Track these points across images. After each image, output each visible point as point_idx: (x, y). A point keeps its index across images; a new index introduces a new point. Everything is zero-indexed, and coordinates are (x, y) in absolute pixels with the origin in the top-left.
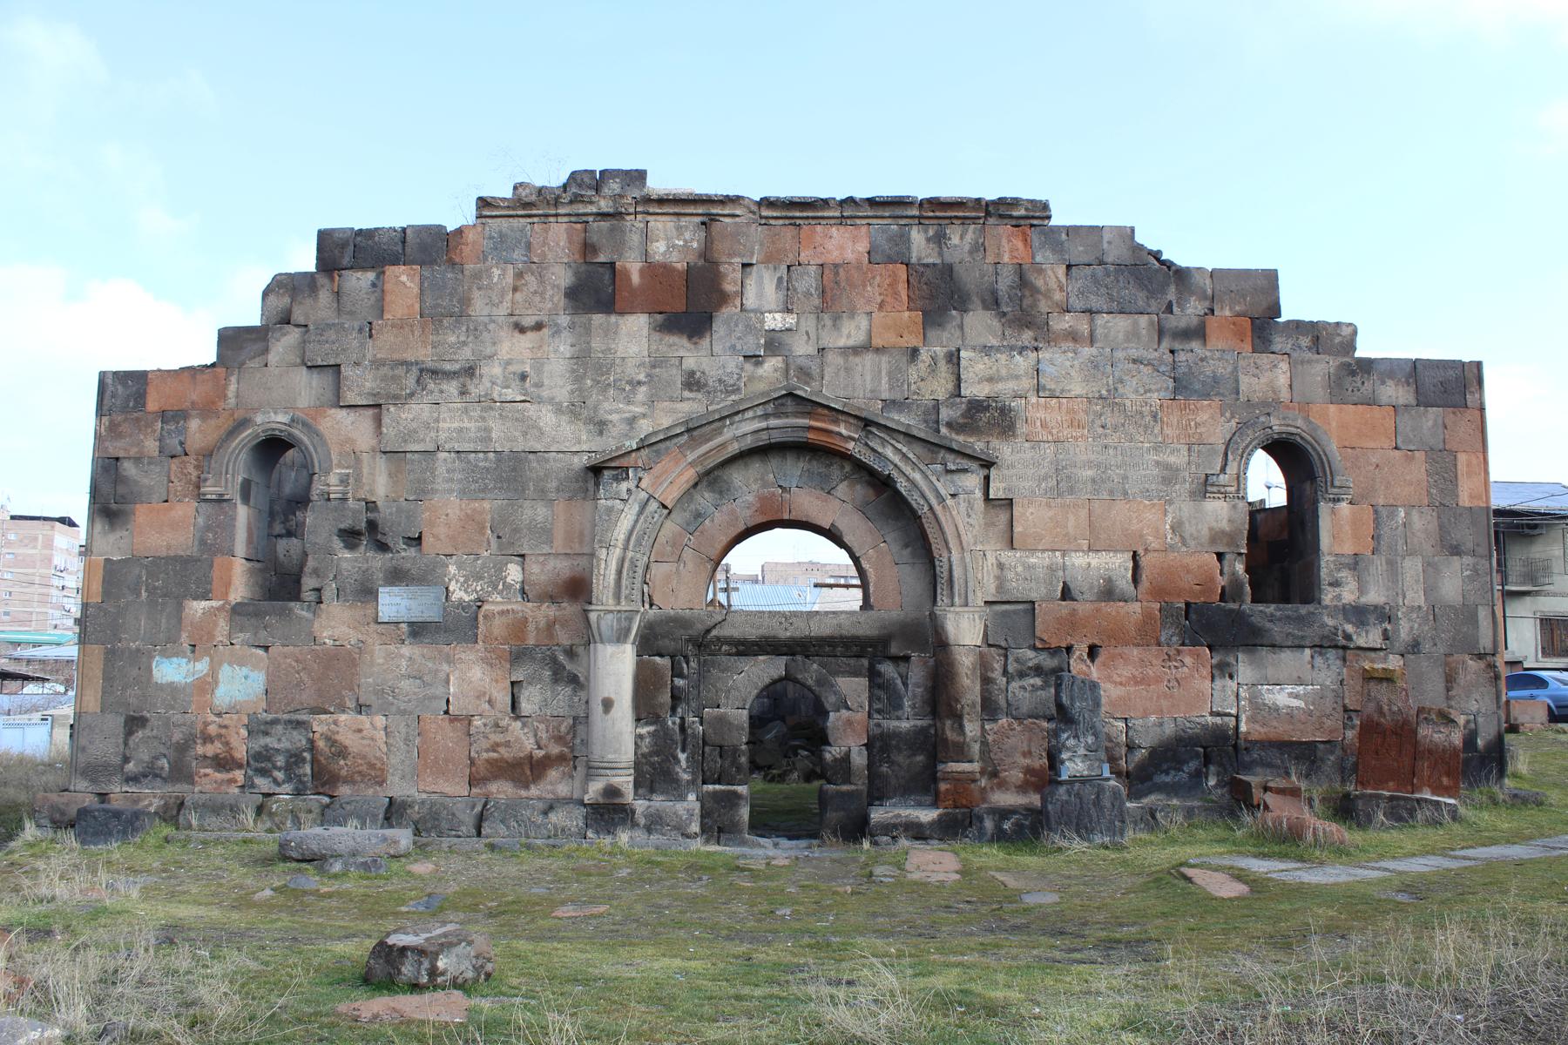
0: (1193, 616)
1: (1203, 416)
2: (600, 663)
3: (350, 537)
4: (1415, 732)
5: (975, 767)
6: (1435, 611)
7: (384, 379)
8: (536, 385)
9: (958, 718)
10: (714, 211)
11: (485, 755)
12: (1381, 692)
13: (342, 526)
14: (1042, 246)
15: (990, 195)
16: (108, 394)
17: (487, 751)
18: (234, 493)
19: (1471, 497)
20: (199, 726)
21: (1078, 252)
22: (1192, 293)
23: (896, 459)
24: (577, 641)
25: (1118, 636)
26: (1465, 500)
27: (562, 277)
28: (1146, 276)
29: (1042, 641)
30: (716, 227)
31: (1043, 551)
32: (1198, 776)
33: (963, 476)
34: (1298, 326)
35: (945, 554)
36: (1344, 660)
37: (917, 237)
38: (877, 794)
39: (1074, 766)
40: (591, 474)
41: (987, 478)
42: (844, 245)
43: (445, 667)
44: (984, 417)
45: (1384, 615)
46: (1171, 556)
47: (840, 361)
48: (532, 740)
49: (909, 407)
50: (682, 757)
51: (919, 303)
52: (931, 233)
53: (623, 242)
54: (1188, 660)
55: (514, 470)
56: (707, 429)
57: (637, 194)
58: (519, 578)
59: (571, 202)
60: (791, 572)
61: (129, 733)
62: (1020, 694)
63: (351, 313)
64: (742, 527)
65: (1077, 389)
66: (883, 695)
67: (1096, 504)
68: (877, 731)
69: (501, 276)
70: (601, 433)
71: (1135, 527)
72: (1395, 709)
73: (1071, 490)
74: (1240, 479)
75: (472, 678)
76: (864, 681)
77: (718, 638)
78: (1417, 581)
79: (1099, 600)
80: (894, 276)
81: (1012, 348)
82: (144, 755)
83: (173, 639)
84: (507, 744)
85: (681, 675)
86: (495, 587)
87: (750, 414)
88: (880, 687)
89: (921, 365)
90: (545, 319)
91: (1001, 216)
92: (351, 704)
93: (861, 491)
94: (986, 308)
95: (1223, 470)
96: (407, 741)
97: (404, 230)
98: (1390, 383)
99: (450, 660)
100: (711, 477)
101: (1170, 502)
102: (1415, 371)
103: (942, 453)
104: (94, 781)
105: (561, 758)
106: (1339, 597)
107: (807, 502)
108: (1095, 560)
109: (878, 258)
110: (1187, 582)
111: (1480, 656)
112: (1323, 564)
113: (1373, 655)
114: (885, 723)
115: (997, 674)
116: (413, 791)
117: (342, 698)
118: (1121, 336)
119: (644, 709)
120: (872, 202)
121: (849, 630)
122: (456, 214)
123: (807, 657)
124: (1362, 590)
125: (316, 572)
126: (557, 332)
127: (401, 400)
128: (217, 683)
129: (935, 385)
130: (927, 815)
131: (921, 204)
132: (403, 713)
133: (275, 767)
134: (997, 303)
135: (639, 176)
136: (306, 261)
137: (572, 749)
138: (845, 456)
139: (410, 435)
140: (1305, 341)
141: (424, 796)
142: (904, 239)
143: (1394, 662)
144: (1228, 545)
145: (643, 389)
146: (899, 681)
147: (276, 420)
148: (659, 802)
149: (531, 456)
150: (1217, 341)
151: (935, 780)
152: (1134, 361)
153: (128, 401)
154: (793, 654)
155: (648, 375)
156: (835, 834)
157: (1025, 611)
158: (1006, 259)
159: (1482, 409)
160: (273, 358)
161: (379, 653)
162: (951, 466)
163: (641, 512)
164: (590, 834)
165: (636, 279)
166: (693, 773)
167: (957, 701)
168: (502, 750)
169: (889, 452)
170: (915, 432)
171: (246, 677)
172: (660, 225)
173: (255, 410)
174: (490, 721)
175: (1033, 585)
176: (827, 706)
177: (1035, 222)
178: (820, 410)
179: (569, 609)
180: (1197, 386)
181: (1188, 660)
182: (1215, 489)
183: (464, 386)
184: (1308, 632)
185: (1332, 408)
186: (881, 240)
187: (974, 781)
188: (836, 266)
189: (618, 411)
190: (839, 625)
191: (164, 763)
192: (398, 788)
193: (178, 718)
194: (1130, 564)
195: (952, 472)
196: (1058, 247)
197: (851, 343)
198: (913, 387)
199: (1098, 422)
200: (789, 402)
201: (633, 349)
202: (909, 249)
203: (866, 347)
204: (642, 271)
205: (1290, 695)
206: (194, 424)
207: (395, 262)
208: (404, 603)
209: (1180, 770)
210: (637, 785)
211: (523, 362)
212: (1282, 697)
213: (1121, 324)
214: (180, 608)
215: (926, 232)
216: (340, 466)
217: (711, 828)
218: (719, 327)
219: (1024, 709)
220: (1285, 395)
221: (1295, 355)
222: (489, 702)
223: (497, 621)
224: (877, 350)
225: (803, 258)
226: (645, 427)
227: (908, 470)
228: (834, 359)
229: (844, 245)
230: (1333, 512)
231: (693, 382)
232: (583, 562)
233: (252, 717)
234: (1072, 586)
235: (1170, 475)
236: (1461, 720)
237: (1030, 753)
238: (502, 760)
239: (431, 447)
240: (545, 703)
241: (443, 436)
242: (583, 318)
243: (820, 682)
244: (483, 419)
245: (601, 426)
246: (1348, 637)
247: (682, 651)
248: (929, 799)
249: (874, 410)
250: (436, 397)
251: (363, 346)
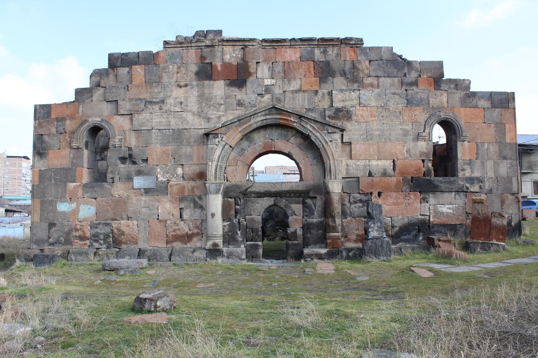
0: (414, 182)
1: (417, 113)
2: (210, 201)
3: (123, 160)
4: (491, 220)
5: (340, 234)
6: (497, 179)
7: (133, 105)
8: (186, 105)
9: (333, 218)
10: (246, 44)
11: (171, 233)
12: (479, 207)
13: (120, 156)
14: (361, 54)
15: (342, 36)
16: (38, 112)
17: (172, 232)
18: (82, 146)
19: (510, 139)
20: (74, 226)
21: (373, 56)
22: (413, 70)
23: (311, 129)
24: (202, 194)
25: (388, 189)
26: (508, 140)
27: (194, 68)
28: (397, 64)
29: (363, 191)
30: (247, 49)
31: (362, 160)
32: (416, 236)
33: (334, 135)
34: (450, 81)
35: (328, 162)
36: (466, 196)
37: (317, 52)
38: (306, 243)
39: (373, 233)
40: (205, 136)
41: (342, 135)
42: (291, 55)
43: (157, 204)
44: (341, 114)
45: (480, 180)
46: (406, 161)
47: (291, 95)
48: (187, 228)
49: (315, 111)
50: (239, 232)
51: (318, 75)
52: (322, 50)
53: (215, 56)
54: (412, 197)
55: (179, 135)
56: (245, 120)
57: (219, 38)
58: (181, 172)
59: (196, 42)
60: (275, 168)
61: (50, 229)
62: (355, 209)
63: (121, 82)
64: (258, 153)
65: (373, 104)
66: (308, 210)
67: (380, 143)
68: (306, 222)
69: (172, 68)
70: (208, 122)
71: (394, 151)
72: (484, 212)
73: (371, 139)
74: (430, 134)
75: (166, 207)
76: (301, 206)
77: (250, 192)
78: (491, 169)
79: (381, 176)
80: (309, 65)
81: (350, 90)
82: (55, 236)
83: (63, 196)
84: (179, 229)
85: (238, 205)
86: (173, 176)
87: (260, 114)
88: (306, 207)
89: (319, 96)
90: (188, 83)
91: (346, 44)
92: (125, 217)
93: (299, 140)
94: (341, 76)
95: (424, 131)
96: (145, 229)
97: (138, 53)
98: (482, 100)
99: (159, 201)
100: (247, 136)
101: (406, 142)
102: (491, 96)
103: (327, 126)
104: (39, 245)
105: (198, 234)
106: (464, 174)
107: (280, 144)
108: (380, 163)
109: (303, 59)
110: (412, 170)
111: (513, 194)
112: (459, 163)
113: (476, 194)
114: (308, 220)
115: (347, 202)
116: (147, 246)
117: (122, 215)
118: (388, 85)
119: (226, 217)
120: (301, 40)
121: (295, 188)
122: (156, 47)
123: (281, 197)
124: (472, 172)
125: (112, 172)
126: (192, 87)
127: (139, 112)
128: (79, 211)
129: (324, 103)
130: (323, 251)
131: (318, 40)
132: (143, 219)
133: (100, 239)
134: (345, 74)
135: (220, 32)
136: (104, 64)
137: (201, 231)
138: (293, 128)
139: (142, 124)
140: (453, 86)
141: (151, 248)
142: (312, 52)
143: (483, 197)
144: (426, 157)
145: (223, 106)
146: (313, 205)
147: (96, 120)
148: (231, 248)
149: (185, 130)
150: (422, 86)
151: (326, 239)
152: (393, 94)
153: (44, 114)
154: (276, 197)
155: (224, 102)
156: (292, 258)
157: (356, 181)
158: (348, 59)
159: (514, 109)
160: (94, 98)
161: (134, 199)
162: (330, 131)
163: (223, 149)
164: (208, 259)
165: (219, 68)
166: (243, 238)
167: (333, 212)
168: (177, 231)
169: (308, 127)
170: (317, 119)
171: (89, 209)
172: (227, 49)
173: (89, 117)
174: (173, 222)
175: (359, 171)
176: (289, 214)
177: (358, 46)
178: (284, 112)
179: (199, 183)
180: (415, 102)
181: (412, 197)
182: (421, 138)
184: (454, 186)
185: (462, 109)
186: (305, 53)
187: (339, 239)
188: (289, 62)
189: (214, 114)
190: (292, 187)
191: (62, 238)
192: (142, 245)
193: (66, 223)
194: (392, 164)
195: (330, 133)
196: (366, 54)
197: (295, 89)
198: (316, 104)
199: (381, 115)
200: (273, 110)
201: (219, 93)
202: (314, 56)
203: (300, 90)
204: (221, 65)
205: (448, 208)
206: (68, 122)
207: (136, 64)
208: (142, 182)
209: (410, 234)
210: (224, 242)
211: (181, 98)
212: (445, 209)
213: (388, 81)
214: (65, 186)
215: (320, 50)
216: (119, 135)
218: (248, 84)
219: (356, 215)
220: (445, 105)
221: (449, 91)
222: (172, 215)
223: (174, 187)
224: (304, 91)
225: (277, 60)
226: (224, 120)
227: (315, 132)
228: (289, 95)
229: (291, 55)
230: (462, 145)
231: (240, 104)
232: (203, 166)
233: (92, 222)
234: (372, 172)
235: (406, 133)
236: (506, 216)
237: (358, 229)
238: (177, 235)
239: (150, 128)
240: (192, 215)
241: (154, 124)
242: (201, 82)
243: (286, 206)
244: (168, 118)
245: (209, 120)
246: (467, 188)
247: (238, 196)
248: (324, 245)
249: (303, 112)
250: (151, 111)
251: (125, 93)
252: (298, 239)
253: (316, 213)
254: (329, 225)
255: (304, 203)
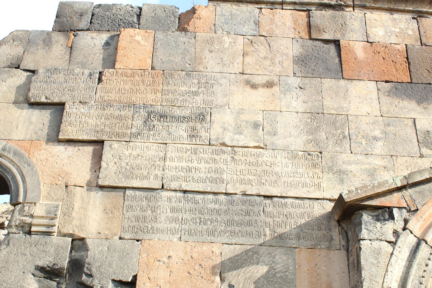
13: (41, 263)
55: (248, 213)
70: (342, 181)
90: (276, 79)
97: (140, 9)
145: (380, 143)
183: (194, 129)
201: (365, 109)
239: (157, 184)
245: (341, 175)
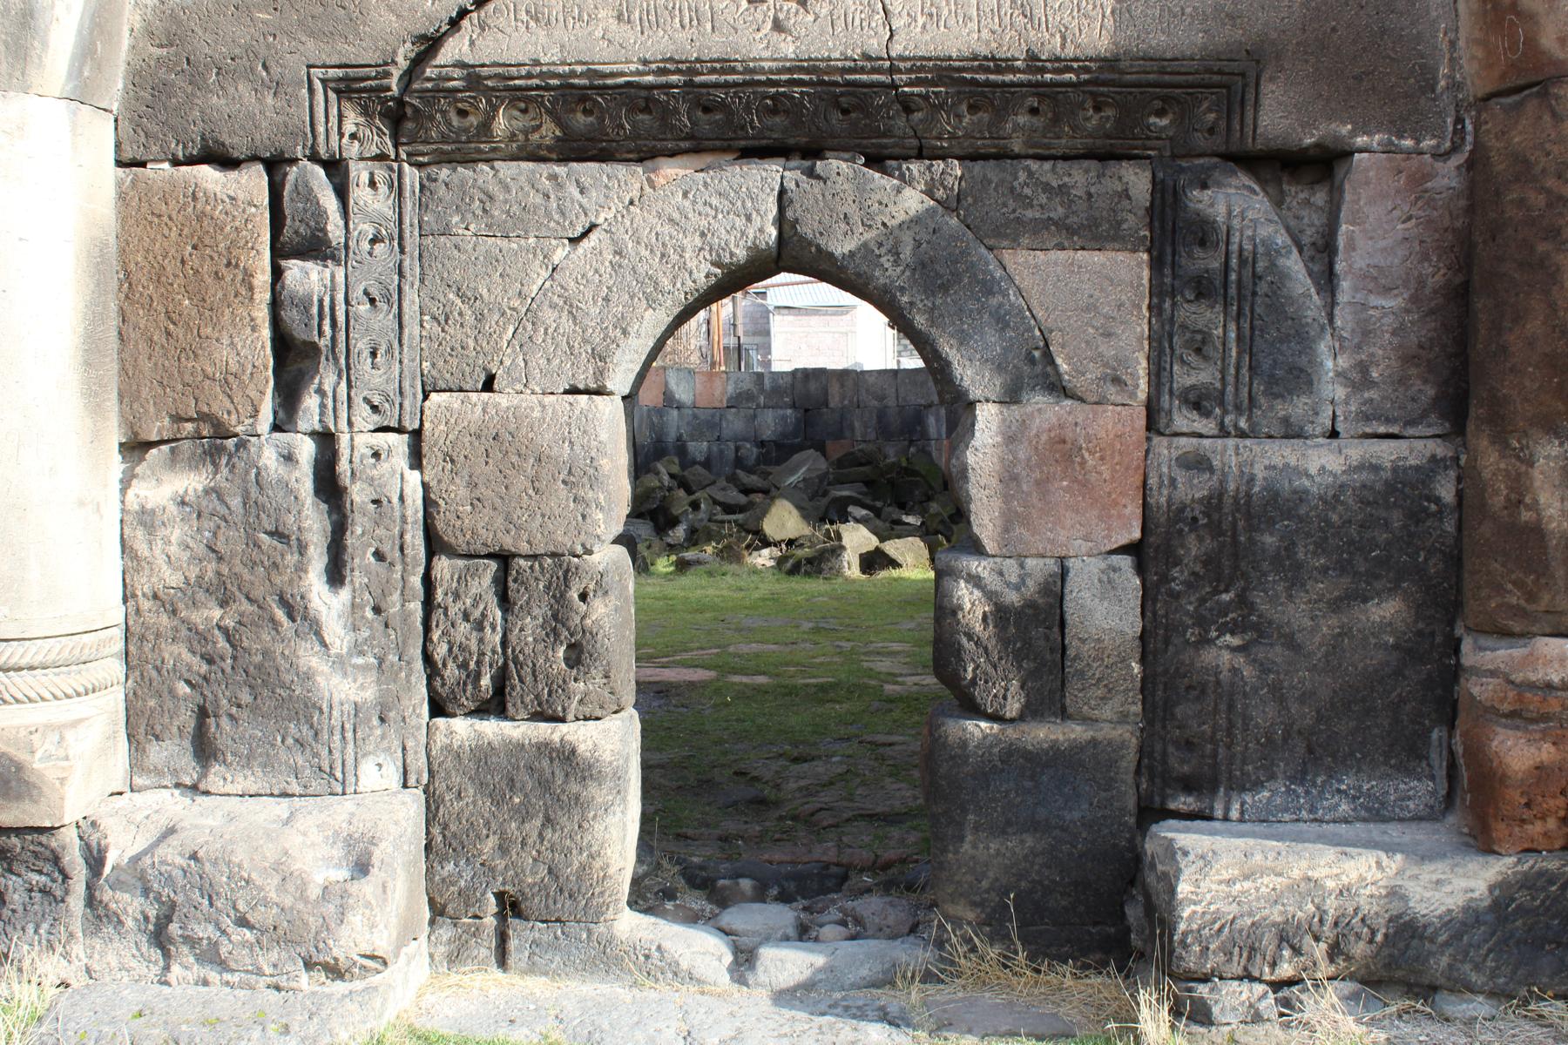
38: (1190, 764)
50: (327, 603)
77: (474, 78)
85: (315, 248)
88: (1203, 289)
114: (1229, 454)
123: (876, 161)
146: (1294, 264)
156: (993, 925)
217: (468, 897)
248: (1420, 790)
252: (1074, 696)
253: (1330, 362)
254: (1536, 531)
255: (1172, 235)
